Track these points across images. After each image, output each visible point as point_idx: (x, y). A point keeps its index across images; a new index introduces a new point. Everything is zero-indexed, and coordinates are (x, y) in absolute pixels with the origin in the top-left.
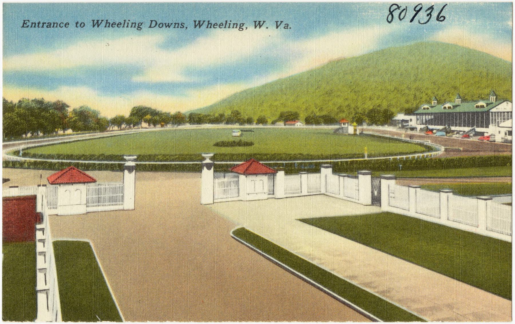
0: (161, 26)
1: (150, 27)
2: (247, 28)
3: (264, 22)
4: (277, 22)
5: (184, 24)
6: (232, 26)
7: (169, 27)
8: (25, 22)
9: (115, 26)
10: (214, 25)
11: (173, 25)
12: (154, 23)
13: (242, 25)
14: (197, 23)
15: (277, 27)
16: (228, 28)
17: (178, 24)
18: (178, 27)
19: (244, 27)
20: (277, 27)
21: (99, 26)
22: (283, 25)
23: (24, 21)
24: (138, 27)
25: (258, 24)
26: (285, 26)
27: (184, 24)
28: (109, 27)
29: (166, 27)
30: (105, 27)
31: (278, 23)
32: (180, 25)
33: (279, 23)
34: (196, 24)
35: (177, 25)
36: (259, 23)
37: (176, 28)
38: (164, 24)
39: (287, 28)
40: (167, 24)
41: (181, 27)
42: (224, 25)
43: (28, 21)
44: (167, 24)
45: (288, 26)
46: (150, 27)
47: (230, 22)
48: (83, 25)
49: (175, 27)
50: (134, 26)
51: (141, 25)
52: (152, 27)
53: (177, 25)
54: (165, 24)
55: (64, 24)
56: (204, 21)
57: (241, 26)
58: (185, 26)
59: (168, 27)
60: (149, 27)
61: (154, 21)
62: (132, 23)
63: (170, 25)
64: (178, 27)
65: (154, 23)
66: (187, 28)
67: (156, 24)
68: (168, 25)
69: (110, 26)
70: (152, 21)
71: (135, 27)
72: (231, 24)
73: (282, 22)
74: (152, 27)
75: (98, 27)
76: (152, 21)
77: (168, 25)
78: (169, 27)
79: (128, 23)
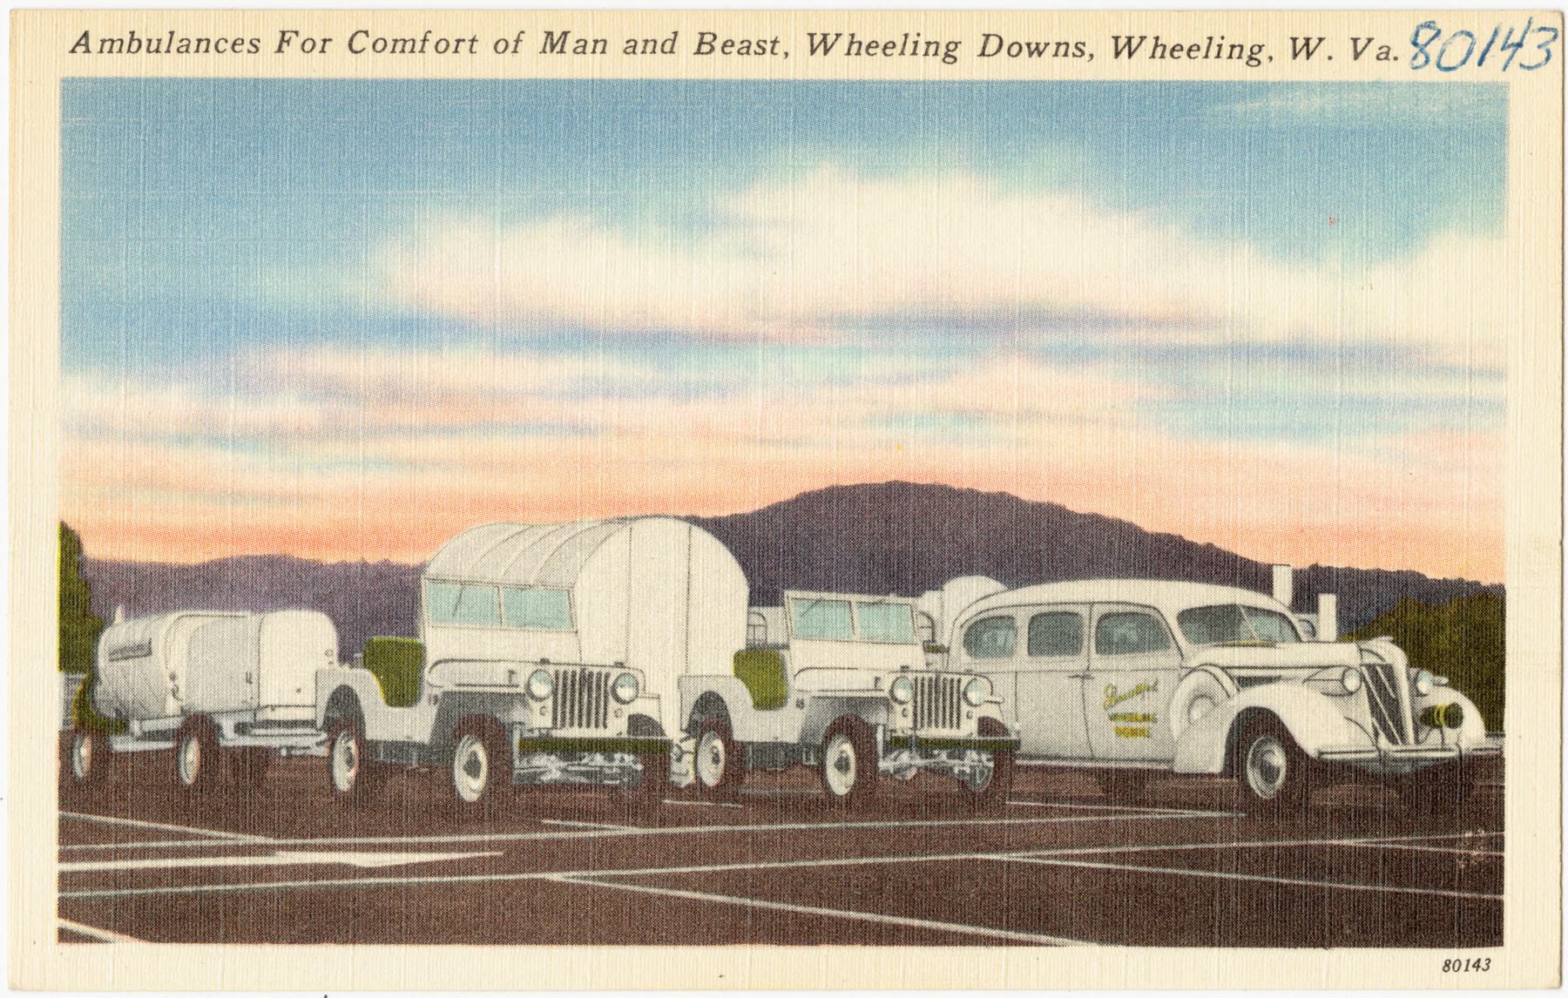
0: (1015, 49)
1: (983, 54)
2: (1271, 58)
3: (1321, 40)
4: (1355, 40)
5: (1084, 44)
6: (1225, 51)
8: (286, 38)
10: (869, 46)
11: (1052, 49)
12: (994, 43)
13: (1256, 49)
14: (1300, 43)
15: (1357, 56)
16: (856, 54)
17: (1067, 44)
18: (1066, 55)
19: (1262, 56)
20: (1357, 56)
21: (1362, 57)
22: (1373, 50)
23: (283, 33)
24: (947, 55)
25: (1305, 45)
26: (1380, 52)
27: (1084, 44)
29: (1031, 54)
30: (1056, 55)
31: (1297, 41)
32: (1072, 49)
33: (1360, 45)
34: (1298, 48)
35: (1062, 49)
36: (1307, 44)
37: (853, 57)
38: (1025, 48)
39: (1386, 58)
40: (1033, 47)
41: (1074, 55)
42: (1203, 50)
43: (294, 34)
44: (1033, 47)
45: (1388, 53)
46: (983, 54)
47: (1221, 42)
48: (501, 46)
50: (1063, 54)
51: (953, 51)
52: (989, 56)
53: (1062, 49)
54: (1029, 45)
55: (1186, 49)
56: (1143, 38)
57: (949, 50)
58: (1087, 51)
59: (1035, 54)
60: (981, 55)
61: (996, 35)
62: (1233, 47)
64: (1066, 55)
65: (994, 43)
66: (1092, 56)
68: (1037, 48)
70: (987, 36)
71: (1240, 57)
73: (1370, 40)
74: (989, 56)
76: (987, 36)
78: (1040, 54)
79: (916, 43)
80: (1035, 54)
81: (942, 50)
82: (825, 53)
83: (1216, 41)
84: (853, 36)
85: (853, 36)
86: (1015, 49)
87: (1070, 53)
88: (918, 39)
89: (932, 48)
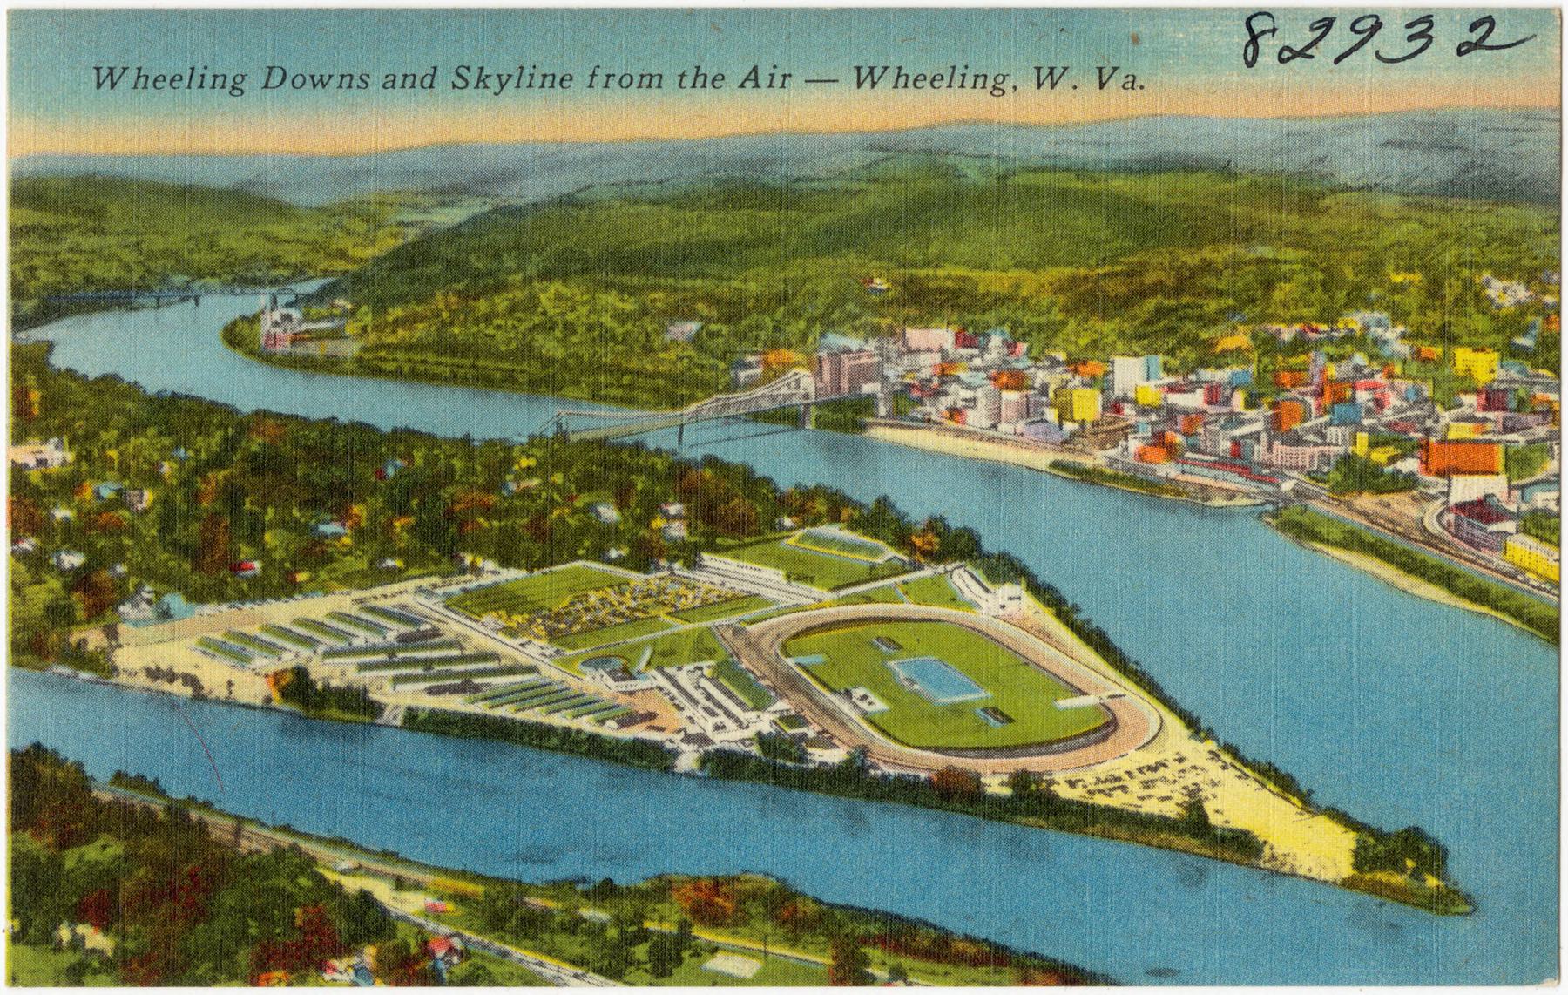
0: (299, 81)
1: (266, 86)
7: (324, 86)
9: (180, 84)
11: (335, 81)
28: (145, 87)
29: (315, 86)
38: (308, 78)
46: (266, 86)
49: (341, 86)
54: (312, 77)
63: (325, 79)
67: (285, 74)
68: (321, 80)
69: (150, 83)
72: (535, 77)
75: (113, 86)
77: (321, 80)
80: (320, 86)
81: (229, 83)
82: (112, 87)
83: (527, 72)
84: (139, 69)
85: (139, 69)
86: (299, 81)
87: (354, 83)
88: (204, 72)
89: (219, 81)
